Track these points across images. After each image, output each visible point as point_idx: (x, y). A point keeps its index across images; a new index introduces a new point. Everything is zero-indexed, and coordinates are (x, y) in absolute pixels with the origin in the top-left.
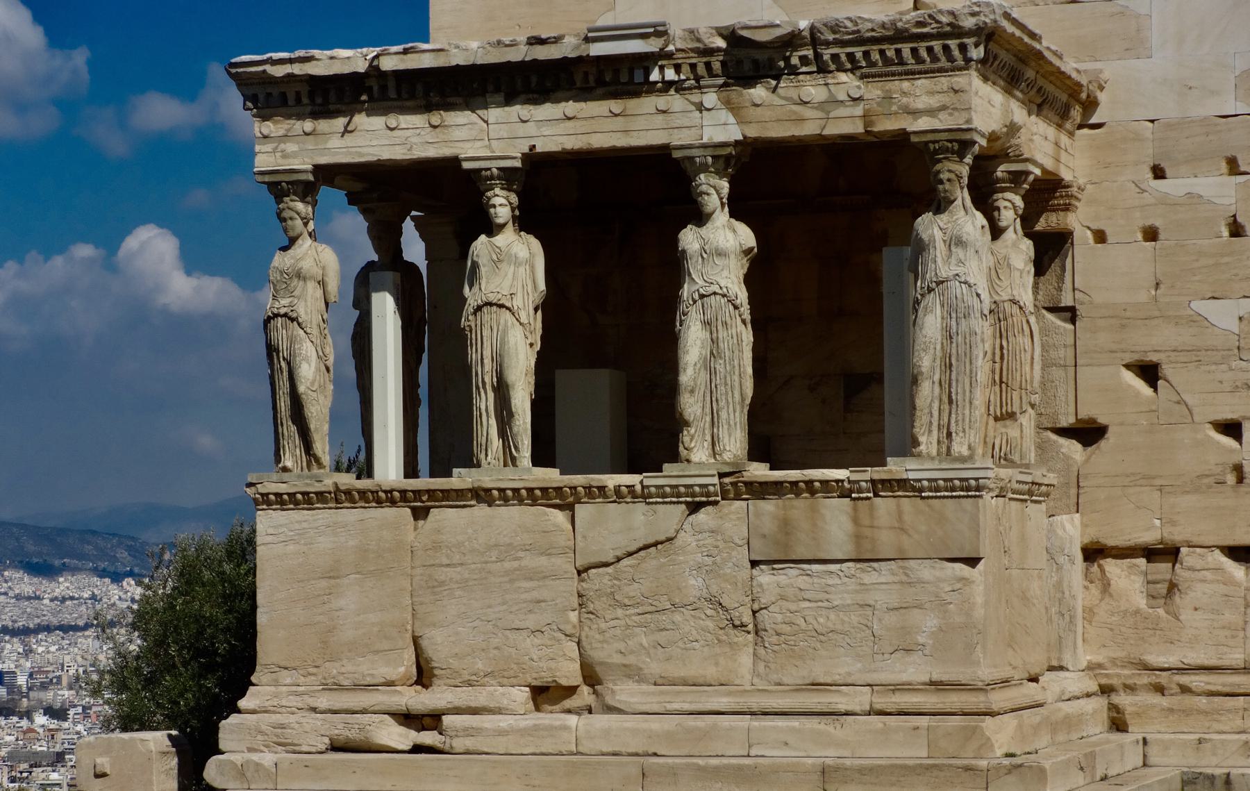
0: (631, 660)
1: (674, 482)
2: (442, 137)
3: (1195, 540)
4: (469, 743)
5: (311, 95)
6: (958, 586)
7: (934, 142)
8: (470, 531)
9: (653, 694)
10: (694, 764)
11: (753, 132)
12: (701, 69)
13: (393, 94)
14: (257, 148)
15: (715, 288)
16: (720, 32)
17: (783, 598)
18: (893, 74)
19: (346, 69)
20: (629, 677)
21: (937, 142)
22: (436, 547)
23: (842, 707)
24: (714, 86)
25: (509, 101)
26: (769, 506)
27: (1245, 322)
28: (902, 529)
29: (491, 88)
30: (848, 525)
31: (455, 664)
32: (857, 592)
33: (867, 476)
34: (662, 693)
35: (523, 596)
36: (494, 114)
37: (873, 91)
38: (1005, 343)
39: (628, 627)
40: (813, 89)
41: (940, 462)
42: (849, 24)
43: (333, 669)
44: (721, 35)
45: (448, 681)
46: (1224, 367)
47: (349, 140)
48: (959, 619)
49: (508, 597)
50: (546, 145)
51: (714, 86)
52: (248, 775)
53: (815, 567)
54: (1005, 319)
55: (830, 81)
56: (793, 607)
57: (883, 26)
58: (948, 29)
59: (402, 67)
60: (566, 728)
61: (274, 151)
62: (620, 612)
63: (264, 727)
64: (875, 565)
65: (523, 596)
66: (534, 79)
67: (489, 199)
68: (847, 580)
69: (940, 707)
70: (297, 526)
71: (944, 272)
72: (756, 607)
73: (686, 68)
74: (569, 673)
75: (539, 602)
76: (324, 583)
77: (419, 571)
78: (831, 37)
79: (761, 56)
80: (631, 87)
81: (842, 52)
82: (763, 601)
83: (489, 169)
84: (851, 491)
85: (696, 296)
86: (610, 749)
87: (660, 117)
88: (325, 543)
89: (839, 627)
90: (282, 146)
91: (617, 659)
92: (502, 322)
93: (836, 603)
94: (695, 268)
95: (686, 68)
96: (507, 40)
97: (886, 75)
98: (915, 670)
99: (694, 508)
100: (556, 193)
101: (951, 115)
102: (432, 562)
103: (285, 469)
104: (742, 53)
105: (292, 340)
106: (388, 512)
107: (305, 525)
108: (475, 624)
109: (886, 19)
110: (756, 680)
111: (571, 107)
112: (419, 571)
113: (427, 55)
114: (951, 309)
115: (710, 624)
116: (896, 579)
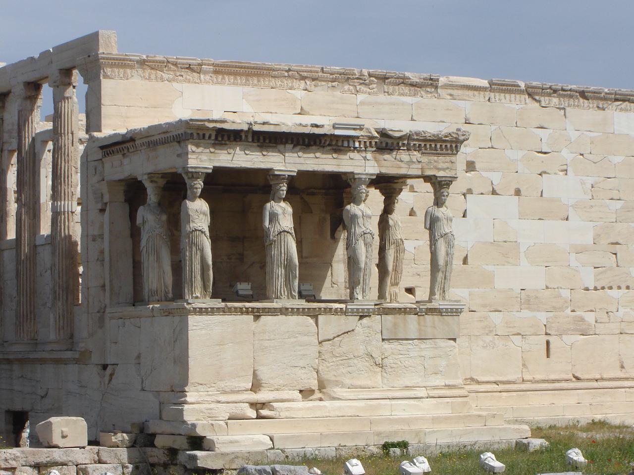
1: (359, 307)
2: (267, 160)
4: (287, 414)
6: (452, 349)
8: (277, 326)
9: (350, 392)
10: (389, 418)
11: (384, 171)
12: (368, 144)
13: (250, 140)
14: (189, 156)
15: (368, 231)
17: (393, 353)
18: (432, 154)
20: (337, 385)
21: (445, 181)
23: (420, 395)
24: (371, 151)
26: (389, 318)
27: (416, 250)
29: (290, 142)
31: (271, 382)
32: (419, 351)
33: (425, 307)
34: (354, 392)
35: (299, 353)
37: (425, 159)
38: (398, 255)
39: (337, 365)
42: (423, 133)
43: (222, 384)
44: (378, 133)
45: (268, 389)
46: (410, 266)
51: (371, 151)
53: (404, 342)
54: (399, 246)
55: (410, 154)
57: (434, 135)
58: (454, 139)
60: (325, 406)
64: (425, 341)
65: (299, 353)
66: (307, 140)
67: (281, 187)
68: (415, 346)
69: (452, 394)
70: (206, 322)
71: (447, 231)
72: (383, 357)
73: (362, 143)
75: (304, 355)
76: (218, 347)
77: (257, 342)
78: (416, 137)
79: (390, 141)
82: (386, 355)
83: (285, 175)
84: (418, 313)
85: (362, 234)
86: (341, 415)
87: (351, 161)
90: (200, 157)
91: (333, 378)
92: (289, 239)
93: (411, 355)
94: (360, 221)
95: (362, 143)
98: (440, 382)
99: (361, 317)
101: (450, 171)
103: (197, 297)
106: (245, 317)
107: (210, 322)
112: (257, 342)
113: (272, 126)
115: (367, 364)
116: (432, 346)
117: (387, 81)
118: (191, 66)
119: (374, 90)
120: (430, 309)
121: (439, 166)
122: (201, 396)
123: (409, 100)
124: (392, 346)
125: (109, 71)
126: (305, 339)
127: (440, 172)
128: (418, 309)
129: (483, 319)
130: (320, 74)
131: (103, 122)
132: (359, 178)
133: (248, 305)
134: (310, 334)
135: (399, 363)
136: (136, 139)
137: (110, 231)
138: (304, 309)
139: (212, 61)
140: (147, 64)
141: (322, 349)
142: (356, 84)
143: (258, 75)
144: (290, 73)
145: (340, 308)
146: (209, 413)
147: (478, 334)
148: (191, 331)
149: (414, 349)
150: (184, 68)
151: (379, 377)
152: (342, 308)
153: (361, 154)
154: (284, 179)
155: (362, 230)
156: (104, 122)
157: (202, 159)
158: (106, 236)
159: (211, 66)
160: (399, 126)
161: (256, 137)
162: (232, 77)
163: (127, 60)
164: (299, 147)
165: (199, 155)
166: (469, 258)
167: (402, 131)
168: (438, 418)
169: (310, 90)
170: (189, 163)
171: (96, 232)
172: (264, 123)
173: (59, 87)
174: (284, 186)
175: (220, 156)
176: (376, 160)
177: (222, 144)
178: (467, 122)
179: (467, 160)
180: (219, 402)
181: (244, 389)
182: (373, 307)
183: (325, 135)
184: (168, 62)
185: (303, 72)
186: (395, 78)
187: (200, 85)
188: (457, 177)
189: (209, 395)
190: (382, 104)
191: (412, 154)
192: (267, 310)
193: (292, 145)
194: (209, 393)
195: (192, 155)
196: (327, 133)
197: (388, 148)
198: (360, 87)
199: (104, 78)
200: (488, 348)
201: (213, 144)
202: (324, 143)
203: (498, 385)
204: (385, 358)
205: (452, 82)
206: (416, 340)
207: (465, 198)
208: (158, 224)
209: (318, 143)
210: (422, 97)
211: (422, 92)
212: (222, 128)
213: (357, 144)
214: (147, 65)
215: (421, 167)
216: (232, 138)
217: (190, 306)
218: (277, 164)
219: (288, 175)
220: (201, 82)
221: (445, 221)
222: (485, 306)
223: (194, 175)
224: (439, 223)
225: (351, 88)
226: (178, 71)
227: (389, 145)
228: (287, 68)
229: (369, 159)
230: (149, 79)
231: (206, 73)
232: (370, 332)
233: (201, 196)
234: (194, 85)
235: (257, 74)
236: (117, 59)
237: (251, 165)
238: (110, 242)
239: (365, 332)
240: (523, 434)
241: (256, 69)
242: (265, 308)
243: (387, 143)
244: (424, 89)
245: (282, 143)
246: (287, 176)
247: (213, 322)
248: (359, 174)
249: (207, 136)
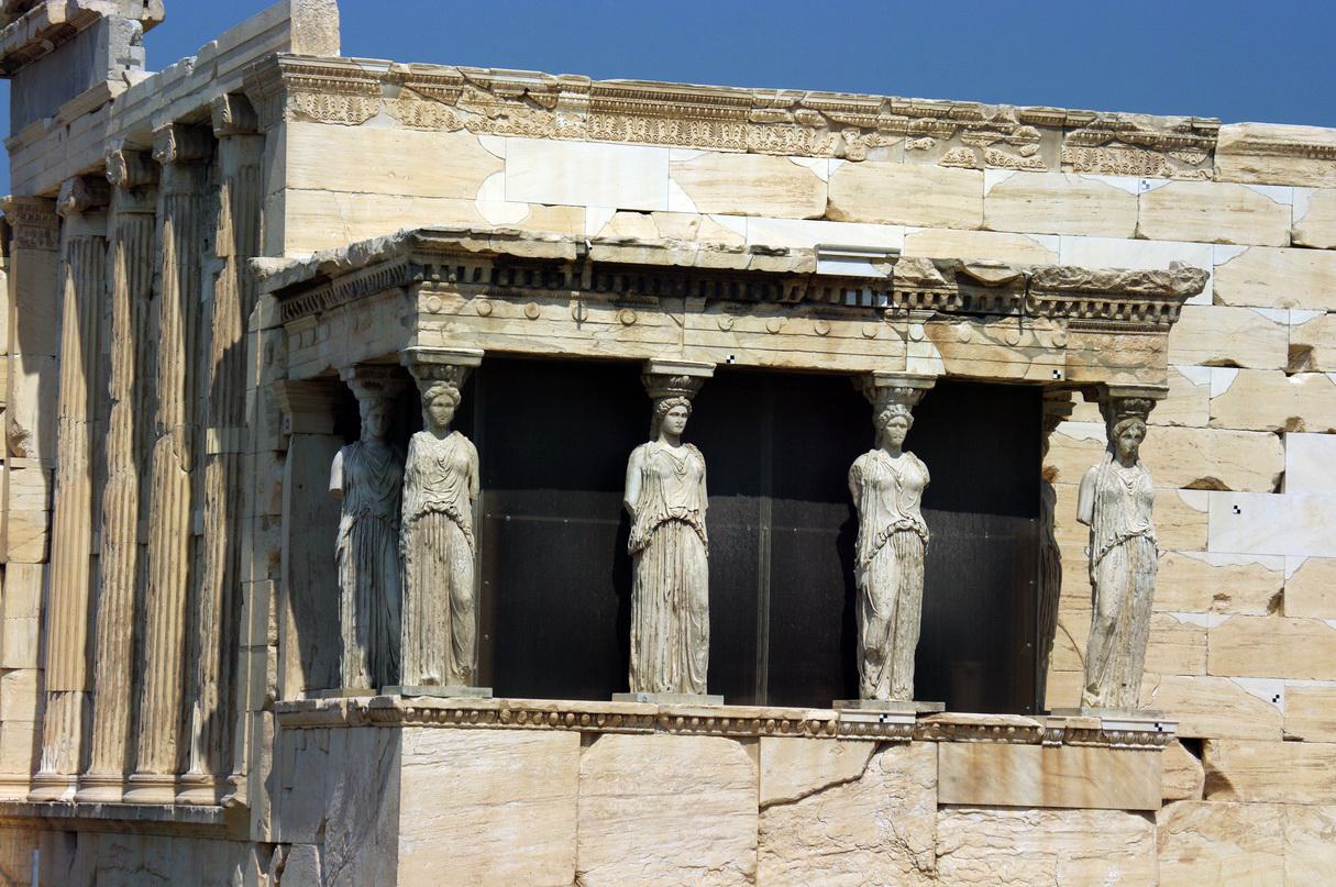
5: (495, 275)
7: (1130, 398)
11: (957, 368)
12: (913, 299)
13: (587, 284)
14: (421, 324)
15: (909, 523)
21: (1133, 398)
22: (610, 775)
25: (707, 308)
26: (959, 750)
28: (1088, 779)
30: (1037, 773)
32: (1040, 839)
33: (1062, 725)
35: (702, 832)
36: (691, 319)
37: (1077, 341)
41: (1132, 714)
42: (1069, 274)
44: (942, 270)
47: (530, 327)
49: (685, 832)
50: (744, 359)
53: (1000, 813)
55: (1035, 326)
58: (1160, 290)
59: (615, 259)
61: (441, 329)
62: (803, 852)
64: (1059, 813)
66: (742, 288)
73: (898, 297)
76: (480, 811)
80: (841, 309)
81: (1054, 298)
83: (682, 376)
84: (1042, 738)
87: (866, 342)
88: (484, 765)
90: (451, 326)
93: (1020, 850)
95: (898, 297)
97: (1090, 327)
99: (882, 746)
100: (732, 408)
101: (1146, 373)
102: (603, 792)
103: (431, 682)
111: (774, 322)
112: (587, 801)
113: (643, 250)
115: (893, 867)
116: (1079, 828)
117: (1068, 134)
118: (529, 93)
119: (1033, 158)
120: (1076, 730)
121: (1118, 358)
123: (1132, 184)
124: (965, 823)
125: (305, 101)
126: (725, 796)
127: (1118, 376)
128: (1041, 731)
129: (1322, 761)
130: (884, 116)
131: (289, 230)
132: (888, 388)
134: (737, 785)
136: (331, 276)
137: (293, 507)
138: (719, 720)
139: (586, 81)
140: (411, 84)
141: (768, 823)
142: (982, 143)
143: (712, 118)
144: (799, 112)
145: (821, 721)
147: (1308, 800)
148: (408, 767)
150: (513, 99)
152: (827, 721)
153: (896, 326)
154: (678, 385)
156: (291, 230)
157: (454, 328)
158: (286, 519)
159: (582, 93)
161: (602, 279)
162: (644, 123)
163: (356, 74)
165: (448, 322)
166: (1286, 599)
167: (1008, 268)
169: (855, 158)
170: (419, 343)
171: (268, 510)
172: (623, 243)
173: (233, 137)
174: (682, 404)
175: (506, 324)
176: (937, 341)
177: (513, 295)
178: (1296, 242)
179: (1292, 342)
182: (913, 720)
183: (790, 275)
184: (467, 81)
185: (835, 110)
186: (1093, 127)
187: (556, 143)
188: (1167, 390)
190: (1053, 195)
191: (1039, 327)
193: (704, 300)
195: (429, 321)
196: (795, 271)
197: (970, 310)
198: (994, 150)
199: (296, 119)
202: (793, 295)
204: (945, 854)
205: (1256, 137)
206: (1035, 812)
208: (379, 493)
209: (774, 297)
210: (1168, 176)
211: (1168, 165)
212: (507, 255)
214: (408, 87)
215: (1063, 362)
216: (537, 279)
217: (408, 703)
218: (660, 348)
219: (690, 376)
220: (558, 135)
221: (1129, 503)
223: (435, 369)
224: (1113, 508)
225: (969, 152)
226: (497, 105)
227: (972, 304)
228: (790, 99)
229: (917, 338)
230: (417, 123)
231: (570, 108)
232: (903, 785)
233: (461, 422)
234: (533, 141)
235: (710, 114)
236: (329, 72)
237: (589, 350)
238: (291, 535)
239: (889, 783)
241: (707, 101)
242: (613, 715)
244: (1177, 155)
245: (675, 294)
246: (686, 378)
247: (468, 746)
248: (888, 376)
249: (469, 273)
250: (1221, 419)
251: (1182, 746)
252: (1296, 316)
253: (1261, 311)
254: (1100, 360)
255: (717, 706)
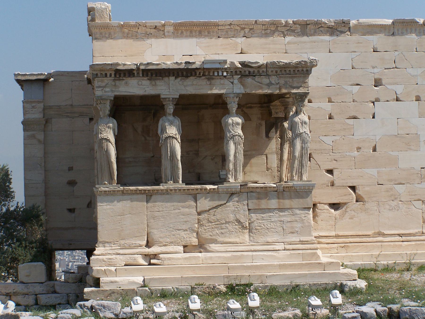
0: (214, 237)
3: (322, 202)
11: (248, 91)
13: (141, 75)
15: (237, 134)
16: (241, 63)
17: (258, 219)
19: (130, 68)
23: (277, 249)
27: (334, 142)
31: (161, 240)
35: (182, 220)
37: (282, 81)
39: (212, 228)
40: (266, 80)
44: (240, 64)
48: (307, 224)
52: (107, 273)
56: (261, 222)
57: (286, 63)
60: (199, 257)
61: (102, 90)
62: (210, 224)
63: (105, 259)
71: (301, 131)
72: (250, 221)
74: (195, 241)
76: (119, 217)
79: (251, 70)
80: (213, 77)
85: (232, 136)
89: (274, 227)
90: (104, 89)
91: (210, 237)
94: (230, 128)
95: (230, 72)
96: (179, 62)
103: (105, 184)
104: (246, 69)
105: (107, 145)
108: (167, 228)
109: (288, 62)
110: (250, 242)
114: (304, 142)
115: (237, 227)
116: (289, 214)
122: (106, 250)
133: (140, 188)
135: (263, 226)
146: (109, 262)
149: (275, 216)
151: (247, 236)
155: (231, 134)
160: (129, 62)
161: (145, 74)
164: (180, 78)
168: (284, 265)
172: (148, 64)
179: (375, 77)
180: (119, 254)
181: (139, 245)
183: (197, 69)
189: (112, 249)
190: (305, 42)
192: (156, 191)
194: (113, 248)
200: (394, 210)
201: (114, 80)
203: (401, 236)
207: (374, 105)
213: (225, 74)
216: (127, 75)
222: (391, 180)
240: (351, 277)
243: (249, 72)
245: (166, 76)
250: (356, 99)
251: (349, 189)
252: (376, 70)
253: (366, 70)
254: (289, 86)
255: (184, 186)
